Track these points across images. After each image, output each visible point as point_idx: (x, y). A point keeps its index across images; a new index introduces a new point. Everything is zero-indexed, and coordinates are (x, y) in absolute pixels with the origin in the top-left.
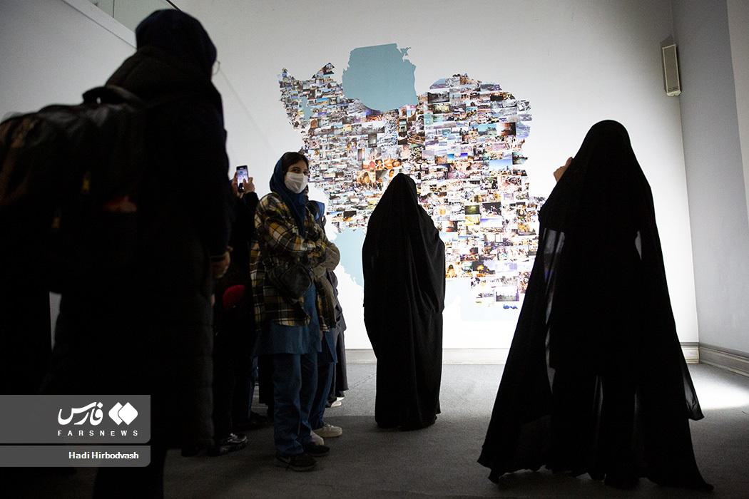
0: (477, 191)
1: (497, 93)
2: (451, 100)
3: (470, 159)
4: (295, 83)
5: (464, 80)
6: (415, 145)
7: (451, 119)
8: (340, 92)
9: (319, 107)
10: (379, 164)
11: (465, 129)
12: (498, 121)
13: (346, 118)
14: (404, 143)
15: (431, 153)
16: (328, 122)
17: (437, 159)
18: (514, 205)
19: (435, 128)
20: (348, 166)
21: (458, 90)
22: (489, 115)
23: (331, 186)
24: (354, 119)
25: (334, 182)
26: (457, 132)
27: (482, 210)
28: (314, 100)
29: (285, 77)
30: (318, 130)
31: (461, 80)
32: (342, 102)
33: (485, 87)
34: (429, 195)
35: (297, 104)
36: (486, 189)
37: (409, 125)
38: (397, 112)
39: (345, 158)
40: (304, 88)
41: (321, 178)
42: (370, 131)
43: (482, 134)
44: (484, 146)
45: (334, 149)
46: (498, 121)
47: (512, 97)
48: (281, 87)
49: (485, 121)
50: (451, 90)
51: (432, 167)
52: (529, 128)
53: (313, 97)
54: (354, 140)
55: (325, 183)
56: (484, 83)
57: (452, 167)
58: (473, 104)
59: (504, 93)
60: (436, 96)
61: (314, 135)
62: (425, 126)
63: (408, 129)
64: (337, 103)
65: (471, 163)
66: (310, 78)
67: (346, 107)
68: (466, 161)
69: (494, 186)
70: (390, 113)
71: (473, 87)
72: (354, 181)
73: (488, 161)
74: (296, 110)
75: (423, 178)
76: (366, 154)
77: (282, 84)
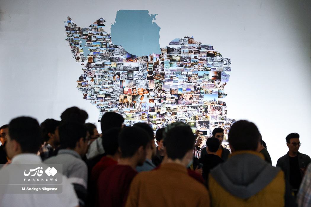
0: (196, 113)
1: (211, 52)
2: (182, 53)
3: (192, 93)
4: (77, 29)
5: (191, 41)
6: (158, 81)
7: (181, 66)
8: (109, 40)
9: (94, 48)
10: (134, 91)
11: (190, 73)
12: (210, 70)
13: (113, 58)
14: (151, 78)
15: (168, 87)
16: (100, 59)
17: (171, 91)
18: (217, 123)
19: (171, 71)
20: (113, 91)
21: (187, 47)
22: (205, 65)
23: (102, 103)
24: (118, 59)
25: (103, 101)
26: (185, 75)
27: (198, 125)
28: (91, 43)
29: (69, 23)
30: (93, 64)
31: (189, 41)
32: (110, 47)
33: (204, 47)
34: (166, 113)
35: (78, 44)
36: (201, 112)
37: (155, 67)
38: (147, 57)
39: (111, 85)
40: (84, 33)
41: (95, 97)
42: (129, 69)
43: (200, 77)
44: (201, 85)
45: (104, 78)
46: (210, 70)
47: (220, 55)
48: (67, 30)
49: (203, 69)
50: (183, 47)
51: (168, 95)
52: (229, 76)
53: (90, 40)
54: (118, 74)
55: (98, 100)
56: (203, 44)
57: (181, 97)
58: (195, 58)
59: (215, 52)
60: (173, 50)
61: (90, 67)
62: (165, 69)
63: (154, 70)
64: (107, 47)
65: (192, 95)
66: (88, 27)
67: (113, 51)
68: (189, 94)
69: (206, 110)
70: (142, 58)
71: (196, 46)
72: (117, 101)
73: (203, 95)
74: (78, 49)
75: (162, 103)
76: (126, 83)
77: (67, 29)
